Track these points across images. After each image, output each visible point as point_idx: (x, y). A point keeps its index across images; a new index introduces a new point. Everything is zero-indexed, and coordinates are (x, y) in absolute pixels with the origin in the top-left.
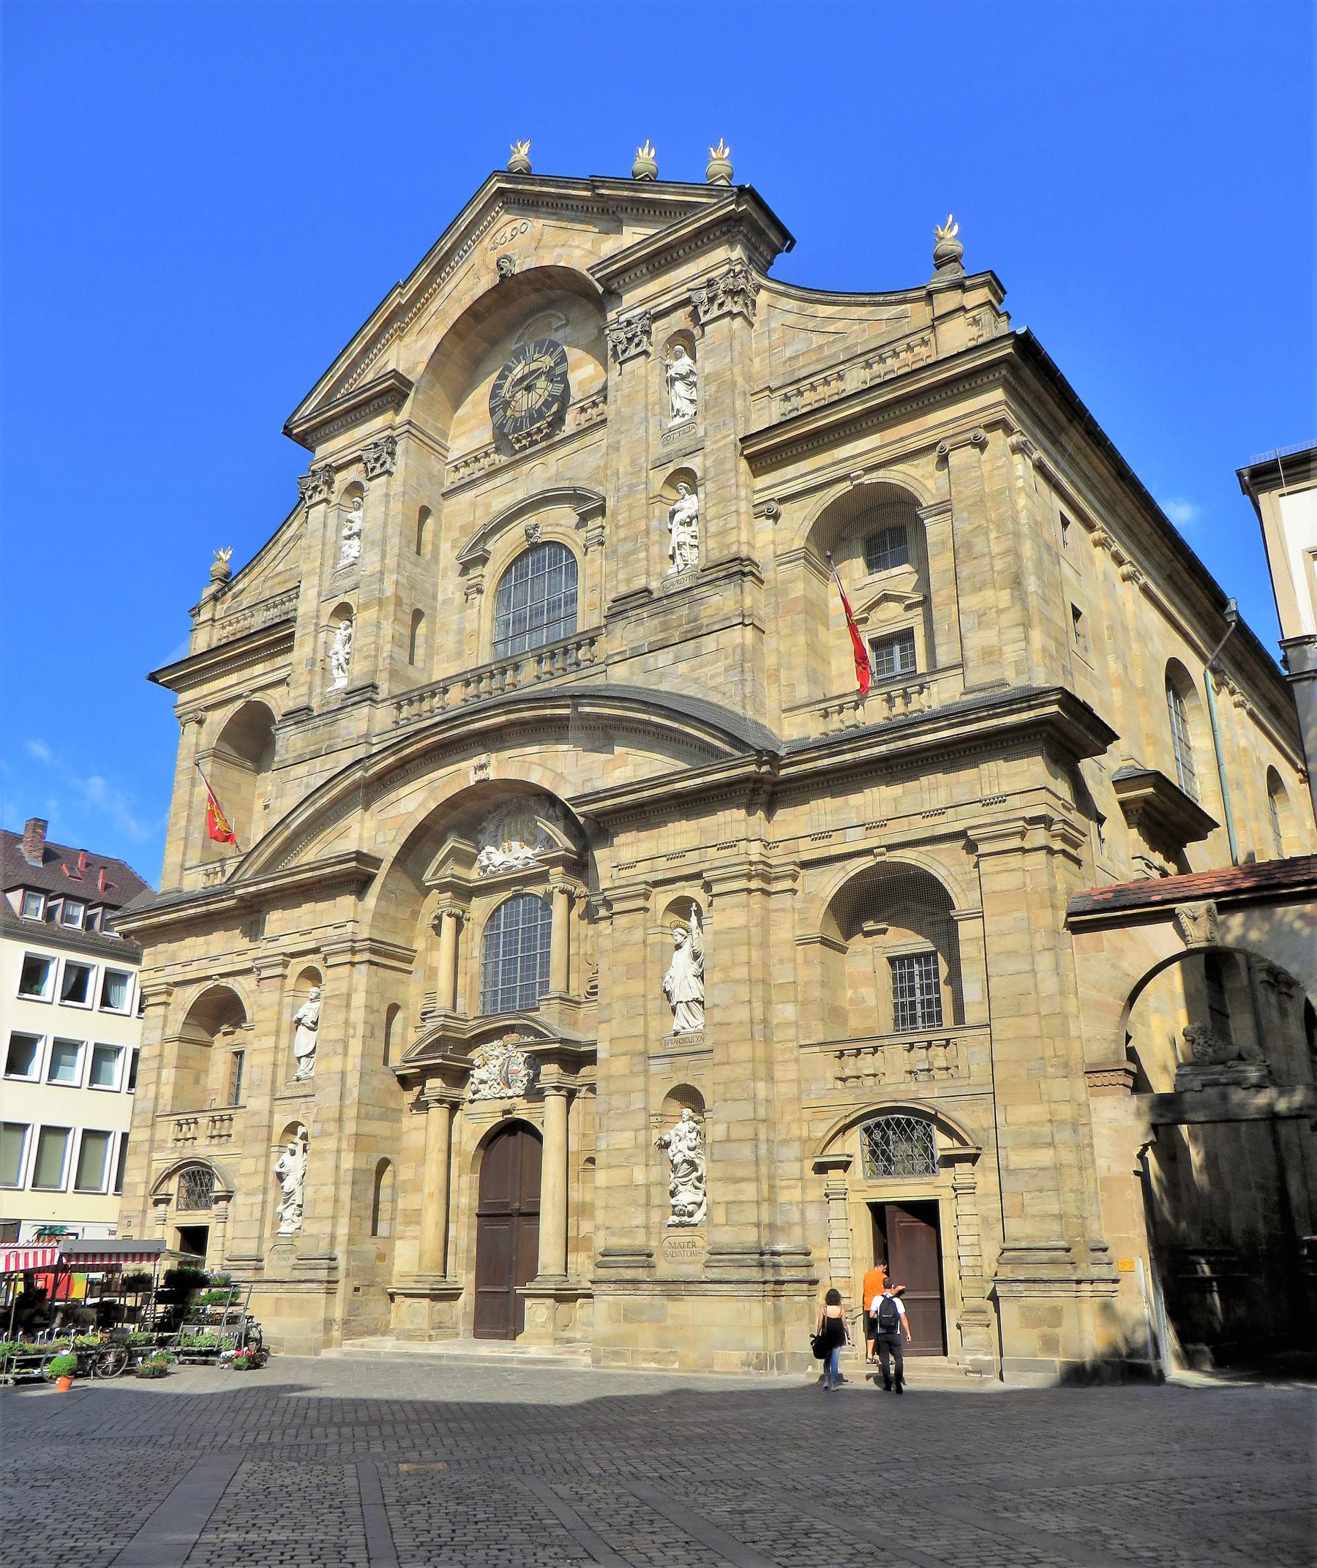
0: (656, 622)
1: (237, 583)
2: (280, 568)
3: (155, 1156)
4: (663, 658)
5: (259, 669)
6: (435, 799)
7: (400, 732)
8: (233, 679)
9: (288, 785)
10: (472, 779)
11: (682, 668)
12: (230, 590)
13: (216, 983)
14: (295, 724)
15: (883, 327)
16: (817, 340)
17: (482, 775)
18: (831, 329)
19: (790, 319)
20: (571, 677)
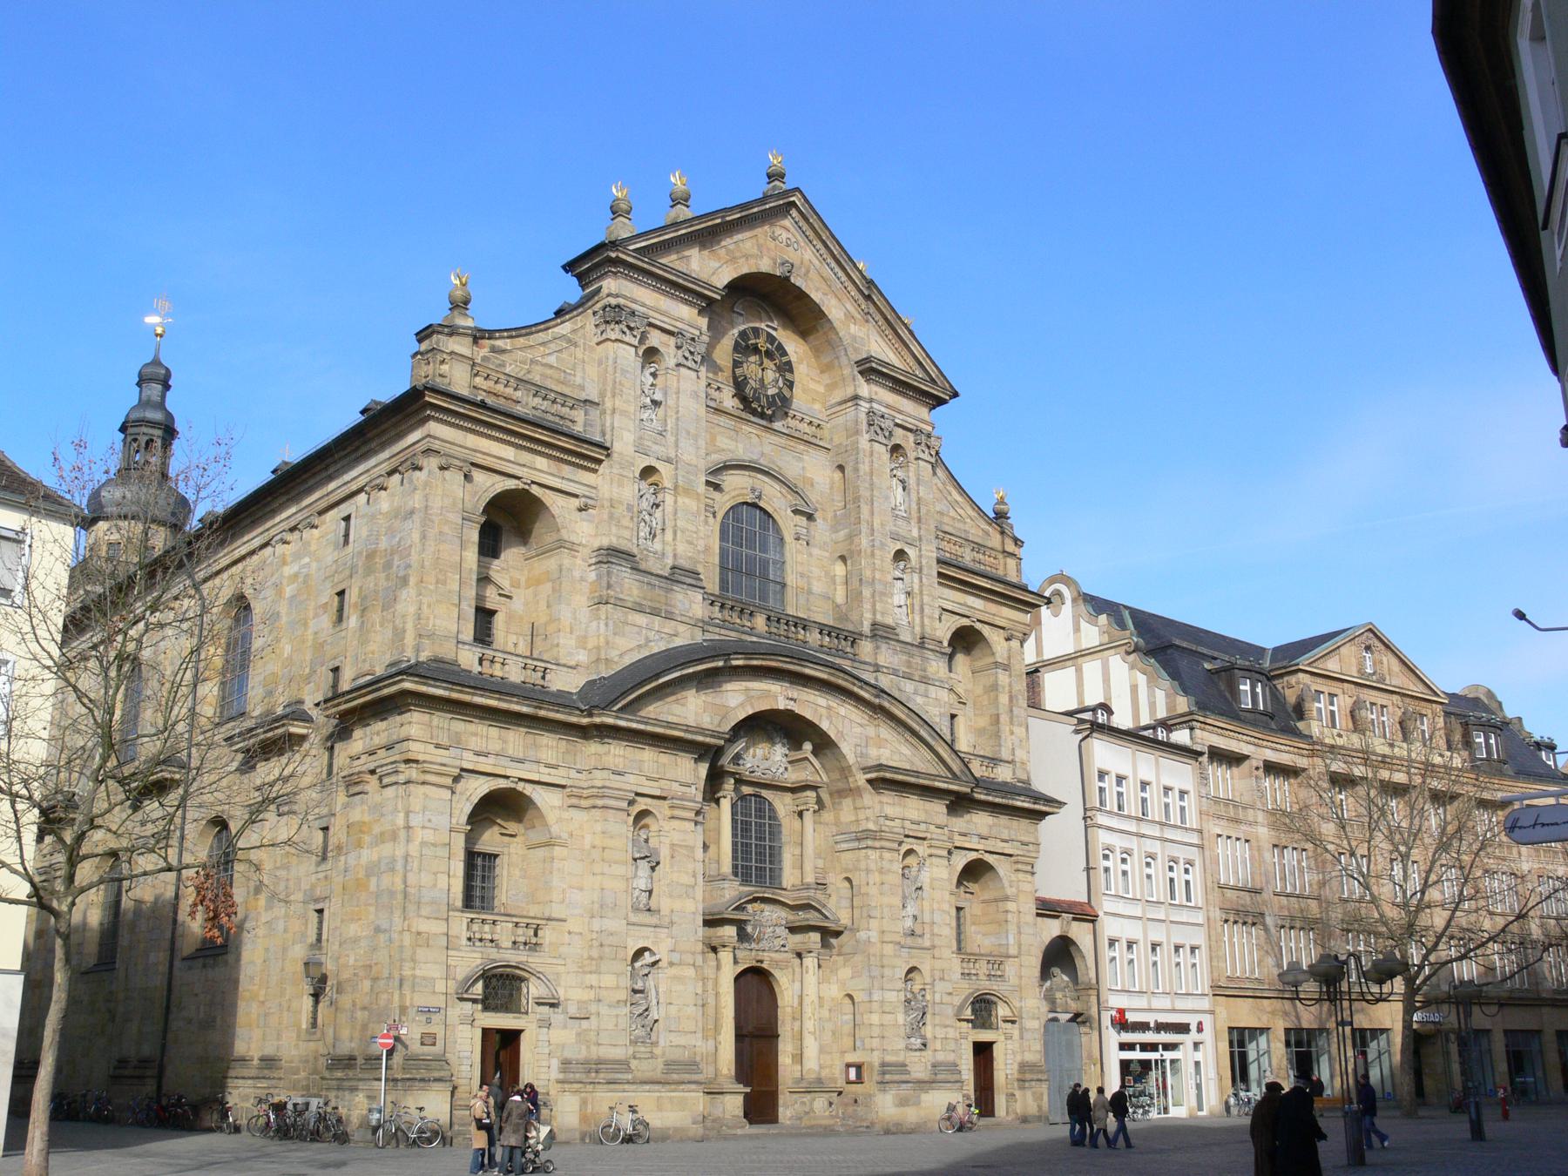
0: (905, 658)
1: (500, 338)
2: (552, 360)
3: (451, 953)
4: (909, 687)
5: (541, 462)
6: (753, 707)
7: (723, 631)
8: (509, 452)
9: (627, 628)
10: (782, 704)
11: (919, 700)
12: (489, 338)
13: (513, 785)
14: (632, 568)
15: (981, 533)
16: (952, 513)
17: (791, 706)
18: (959, 510)
19: (940, 485)
20: (848, 663)
